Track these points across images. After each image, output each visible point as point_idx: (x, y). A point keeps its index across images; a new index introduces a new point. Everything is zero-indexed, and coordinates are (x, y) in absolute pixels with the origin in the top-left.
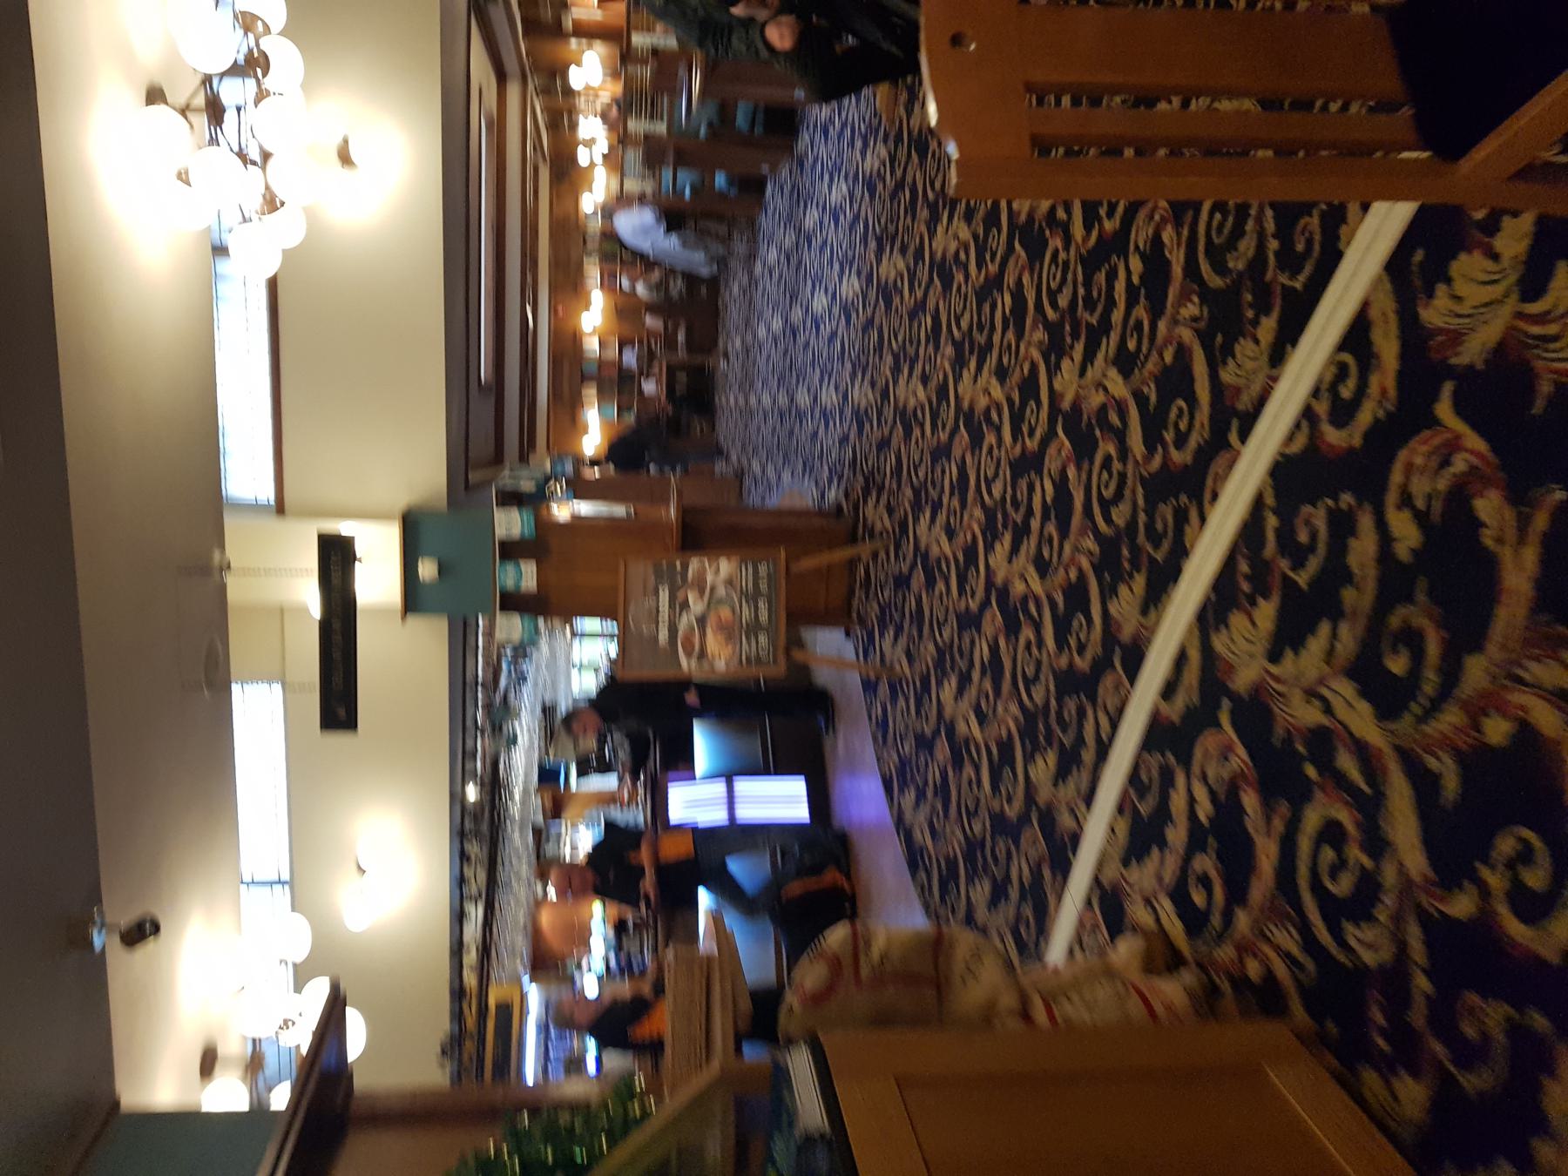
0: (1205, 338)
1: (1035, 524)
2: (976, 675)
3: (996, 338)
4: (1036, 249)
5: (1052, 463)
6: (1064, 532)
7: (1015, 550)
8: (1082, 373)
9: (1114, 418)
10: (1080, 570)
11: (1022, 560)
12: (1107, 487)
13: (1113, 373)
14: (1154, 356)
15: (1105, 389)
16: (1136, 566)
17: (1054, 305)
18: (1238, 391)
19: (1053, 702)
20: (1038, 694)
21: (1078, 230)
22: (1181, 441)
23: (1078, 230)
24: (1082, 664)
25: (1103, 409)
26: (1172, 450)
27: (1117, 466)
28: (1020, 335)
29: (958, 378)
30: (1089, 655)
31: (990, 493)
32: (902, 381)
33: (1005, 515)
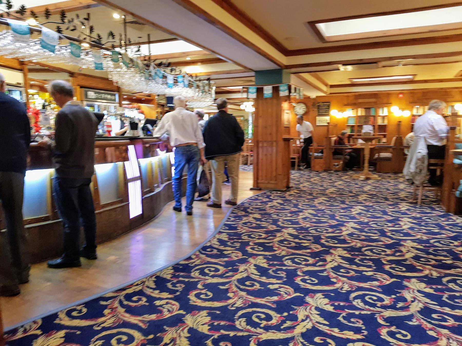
1: (354, 267)
2: (297, 240)
6: (350, 278)
7: (343, 258)
9: (400, 305)
12: (370, 298)
13: (421, 305)
15: (413, 302)
16: (336, 308)
17: (449, 282)
19: (284, 268)
20: (288, 263)
24: (298, 280)
25: (405, 300)
27: (379, 304)
30: (301, 283)
33: (358, 255)
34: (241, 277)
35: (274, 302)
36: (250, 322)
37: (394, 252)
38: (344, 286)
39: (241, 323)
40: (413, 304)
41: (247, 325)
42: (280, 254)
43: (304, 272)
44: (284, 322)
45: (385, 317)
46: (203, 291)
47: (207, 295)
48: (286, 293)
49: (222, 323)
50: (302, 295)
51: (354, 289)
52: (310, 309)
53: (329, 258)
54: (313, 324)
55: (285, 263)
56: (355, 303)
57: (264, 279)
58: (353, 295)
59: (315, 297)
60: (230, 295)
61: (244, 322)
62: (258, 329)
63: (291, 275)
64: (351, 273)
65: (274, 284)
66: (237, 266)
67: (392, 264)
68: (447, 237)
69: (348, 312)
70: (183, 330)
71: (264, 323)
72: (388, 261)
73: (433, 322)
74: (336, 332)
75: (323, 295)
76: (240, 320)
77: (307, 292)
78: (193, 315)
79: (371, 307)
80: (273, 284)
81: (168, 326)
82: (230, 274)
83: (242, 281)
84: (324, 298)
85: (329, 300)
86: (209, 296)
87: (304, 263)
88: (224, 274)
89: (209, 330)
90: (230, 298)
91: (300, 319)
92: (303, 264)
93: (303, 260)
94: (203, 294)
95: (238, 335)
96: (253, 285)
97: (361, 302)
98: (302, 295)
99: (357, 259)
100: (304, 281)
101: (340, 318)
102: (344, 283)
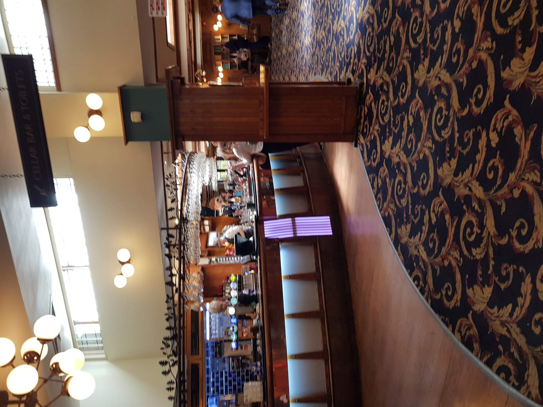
0: (494, 57)
1: (404, 134)
3: (387, 55)
4: (406, 17)
5: (413, 108)
6: (418, 139)
8: (428, 72)
9: (444, 91)
13: (444, 72)
14: (466, 65)
15: (440, 79)
16: (452, 156)
18: (510, 82)
19: (410, 207)
20: (404, 202)
21: (427, 8)
22: (479, 103)
23: (427, 8)
24: (424, 192)
27: (445, 112)
28: (398, 54)
29: (368, 72)
31: (383, 120)
32: (343, 73)
33: (390, 130)
34: (425, 253)
35: (452, 217)
36: (477, 243)
37: (383, 92)
38: (428, 146)
39: (478, 253)
40: (442, 79)
41: (480, 247)
42: (394, 211)
44: (473, 209)
45: (460, 107)
46: (444, 292)
47: (448, 288)
49: (480, 272)
50: (441, 189)
51: (431, 136)
52: (457, 182)
53: (396, 160)
54: (474, 179)
55: (404, 205)
56: (446, 137)
58: (437, 137)
59: (442, 175)
60: (446, 263)
61: (476, 249)
62: (483, 236)
63: (416, 199)
64: (412, 138)
66: (411, 256)
67: (398, 95)
68: (362, 39)
69: (457, 144)
70: (492, 314)
71: (476, 229)
72: (395, 98)
73: (461, 62)
74: (480, 157)
75: (439, 168)
77: (437, 184)
78: (474, 303)
79: (449, 121)
80: (430, 219)
81: (488, 331)
82: (421, 263)
83: (429, 252)
85: (445, 163)
86: (448, 286)
87: (403, 186)
88: (422, 270)
89: (489, 286)
90: (450, 263)
91: (469, 193)
92: (404, 187)
93: (399, 187)
94: (447, 293)
95: (493, 256)
96: (433, 240)
97: (445, 130)
98: (441, 189)
99: (395, 131)
100: (424, 187)
102: (424, 146)
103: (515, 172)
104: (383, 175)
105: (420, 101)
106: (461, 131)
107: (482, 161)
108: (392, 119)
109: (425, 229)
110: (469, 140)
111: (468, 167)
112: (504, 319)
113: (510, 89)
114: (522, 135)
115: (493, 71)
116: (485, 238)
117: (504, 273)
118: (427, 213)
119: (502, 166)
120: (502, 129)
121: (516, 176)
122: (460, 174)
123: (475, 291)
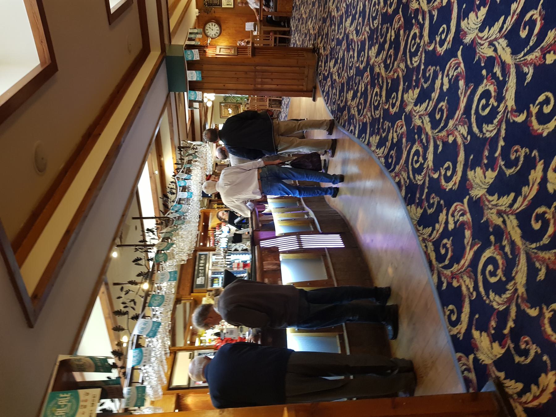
10: (398, 76)
11: (379, 59)
12: (413, 48)
24: (393, 111)
26: (438, 46)
27: (418, 40)
43: (386, 103)
48: (401, 129)
57: (388, 144)
65: (393, 136)
74: (435, 95)
76: (417, 179)
84: (408, 93)
91: (421, 125)
96: (392, 157)
101: (425, 86)
103: (453, 120)
104: (366, 81)
105: (402, 19)
106: (426, 65)
107: (435, 100)
108: (380, 27)
109: (388, 144)
110: (430, 75)
111: (425, 101)
112: (425, 236)
113: (464, 41)
114: (463, 90)
115: (456, 17)
116: (425, 169)
117: (431, 202)
118: (391, 131)
119: (447, 111)
120: (453, 76)
121: (453, 124)
122: (419, 105)
123: (412, 209)
